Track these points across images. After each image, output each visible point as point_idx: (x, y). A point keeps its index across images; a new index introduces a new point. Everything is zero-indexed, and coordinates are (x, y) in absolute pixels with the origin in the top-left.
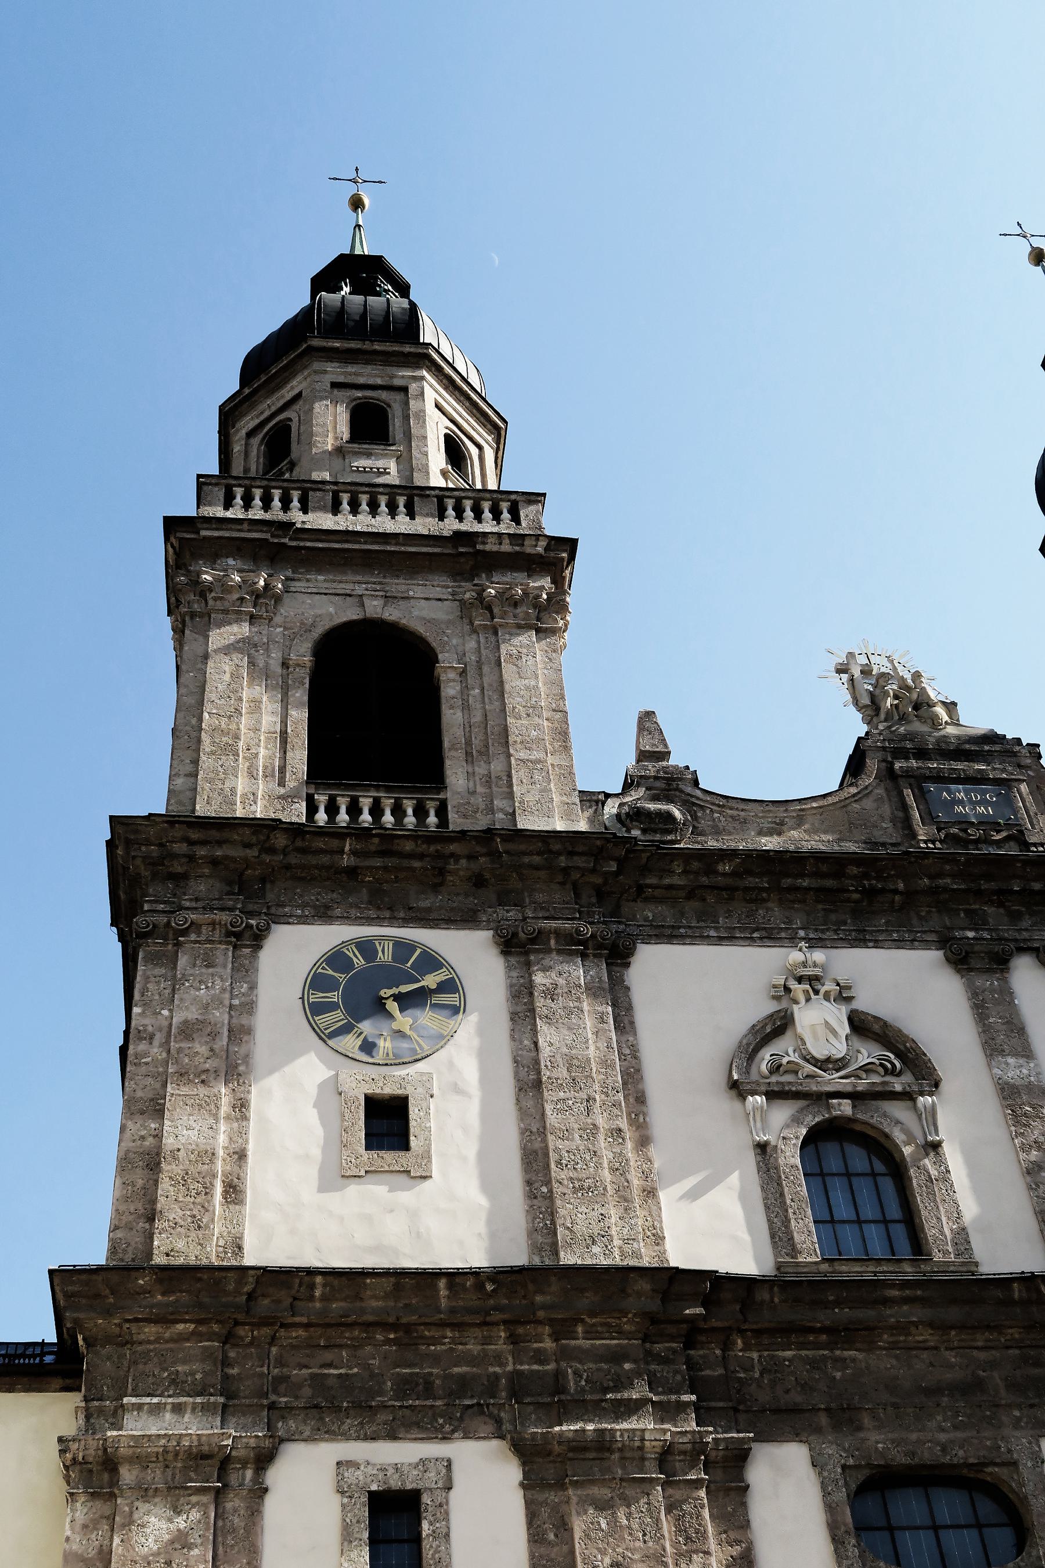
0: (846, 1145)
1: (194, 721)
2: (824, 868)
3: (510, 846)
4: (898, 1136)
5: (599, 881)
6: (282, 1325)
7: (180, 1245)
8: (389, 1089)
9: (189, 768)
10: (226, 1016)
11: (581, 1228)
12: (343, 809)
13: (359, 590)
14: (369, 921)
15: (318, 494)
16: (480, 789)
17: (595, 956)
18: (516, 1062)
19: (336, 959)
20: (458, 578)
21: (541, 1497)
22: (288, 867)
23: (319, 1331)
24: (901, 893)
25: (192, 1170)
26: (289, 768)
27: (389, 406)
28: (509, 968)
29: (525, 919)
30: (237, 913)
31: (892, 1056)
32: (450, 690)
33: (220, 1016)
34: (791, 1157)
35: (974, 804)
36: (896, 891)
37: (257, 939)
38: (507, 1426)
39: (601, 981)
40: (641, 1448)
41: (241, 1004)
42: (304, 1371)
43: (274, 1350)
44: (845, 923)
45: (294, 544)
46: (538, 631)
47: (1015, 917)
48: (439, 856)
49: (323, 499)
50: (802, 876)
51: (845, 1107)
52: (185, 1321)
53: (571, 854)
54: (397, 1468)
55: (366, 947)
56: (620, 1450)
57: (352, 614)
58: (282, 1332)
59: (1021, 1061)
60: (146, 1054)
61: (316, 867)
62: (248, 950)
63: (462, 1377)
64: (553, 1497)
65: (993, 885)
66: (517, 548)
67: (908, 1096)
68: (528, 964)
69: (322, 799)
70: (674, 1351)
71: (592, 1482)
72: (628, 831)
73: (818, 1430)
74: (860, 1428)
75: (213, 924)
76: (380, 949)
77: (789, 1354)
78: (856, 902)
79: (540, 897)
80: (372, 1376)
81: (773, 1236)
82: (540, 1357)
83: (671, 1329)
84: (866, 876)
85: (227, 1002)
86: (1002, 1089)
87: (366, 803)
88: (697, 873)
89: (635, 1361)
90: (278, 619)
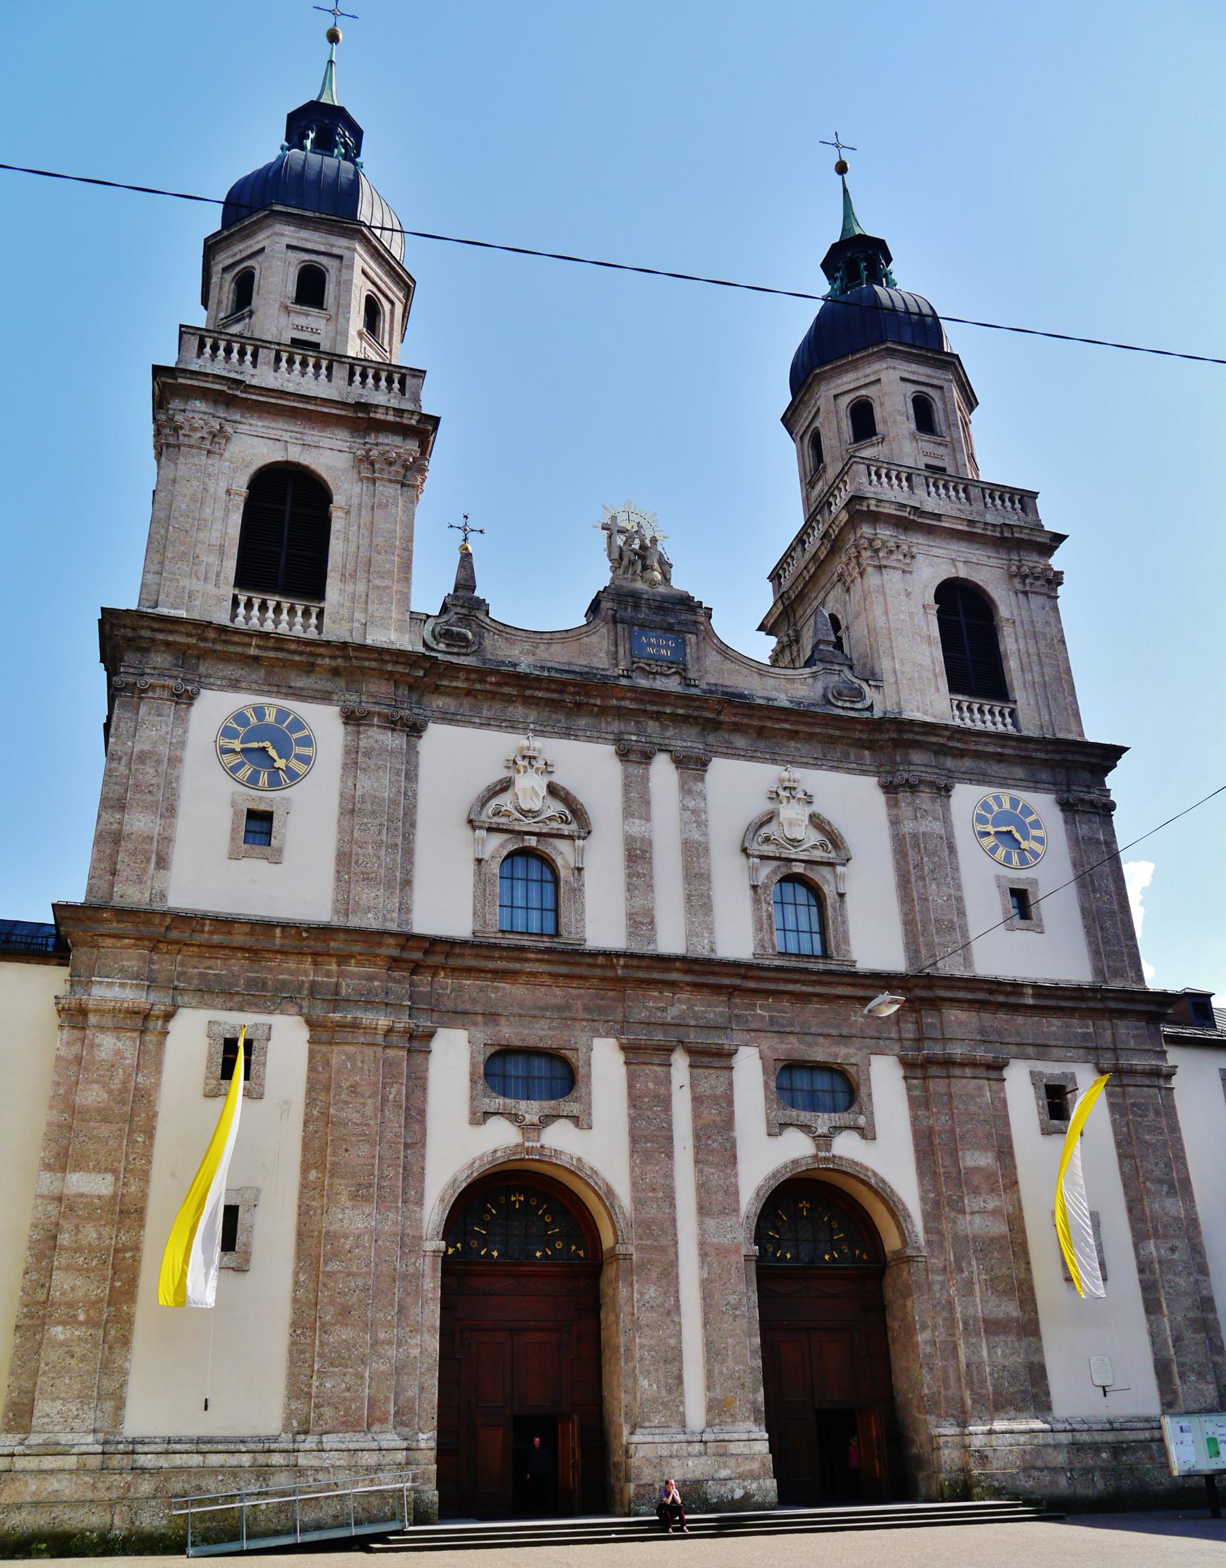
0: (530, 860)
1: (162, 531)
2: (553, 686)
3: (357, 654)
4: (559, 862)
5: (412, 681)
6: (185, 944)
7: (130, 891)
8: (262, 807)
9: (157, 568)
10: (167, 750)
11: (364, 903)
12: (256, 607)
13: (286, 436)
14: (262, 693)
15: (265, 351)
16: (347, 604)
17: (401, 731)
18: (341, 796)
19: (240, 718)
20: (355, 434)
21: (317, 1047)
22: (215, 651)
23: (206, 949)
24: (598, 706)
25: (139, 847)
26: (222, 575)
27: (328, 271)
28: (347, 734)
29: (361, 702)
30: (180, 681)
32: (337, 524)
33: (164, 750)
34: (495, 868)
36: (595, 705)
37: (191, 698)
38: (305, 1010)
39: (401, 749)
40: (376, 1029)
41: (178, 742)
42: (196, 970)
43: (179, 957)
44: (560, 721)
45: (244, 395)
46: (403, 485)
47: (664, 728)
48: (312, 654)
49: (268, 355)
50: (539, 689)
51: (532, 842)
52: (130, 938)
53: (396, 663)
55: (259, 711)
56: (364, 1028)
57: (278, 456)
58: (185, 948)
59: (643, 822)
60: (116, 770)
61: (233, 653)
62: (184, 706)
63: (284, 980)
64: (324, 1048)
65: (655, 708)
66: (398, 419)
67: (570, 837)
68: (359, 732)
69: (243, 599)
70: (404, 977)
71: (347, 1043)
72: (437, 644)
73: (476, 1024)
74: (498, 1025)
75: (164, 686)
76: (267, 713)
77: (468, 982)
78: (570, 708)
79: (373, 688)
80: (233, 976)
81: (474, 914)
82: (328, 974)
83: (404, 965)
84: (578, 693)
85: (168, 741)
86: (627, 839)
87: (271, 604)
88: (474, 681)
89: (381, 981)
90: (227, 455)
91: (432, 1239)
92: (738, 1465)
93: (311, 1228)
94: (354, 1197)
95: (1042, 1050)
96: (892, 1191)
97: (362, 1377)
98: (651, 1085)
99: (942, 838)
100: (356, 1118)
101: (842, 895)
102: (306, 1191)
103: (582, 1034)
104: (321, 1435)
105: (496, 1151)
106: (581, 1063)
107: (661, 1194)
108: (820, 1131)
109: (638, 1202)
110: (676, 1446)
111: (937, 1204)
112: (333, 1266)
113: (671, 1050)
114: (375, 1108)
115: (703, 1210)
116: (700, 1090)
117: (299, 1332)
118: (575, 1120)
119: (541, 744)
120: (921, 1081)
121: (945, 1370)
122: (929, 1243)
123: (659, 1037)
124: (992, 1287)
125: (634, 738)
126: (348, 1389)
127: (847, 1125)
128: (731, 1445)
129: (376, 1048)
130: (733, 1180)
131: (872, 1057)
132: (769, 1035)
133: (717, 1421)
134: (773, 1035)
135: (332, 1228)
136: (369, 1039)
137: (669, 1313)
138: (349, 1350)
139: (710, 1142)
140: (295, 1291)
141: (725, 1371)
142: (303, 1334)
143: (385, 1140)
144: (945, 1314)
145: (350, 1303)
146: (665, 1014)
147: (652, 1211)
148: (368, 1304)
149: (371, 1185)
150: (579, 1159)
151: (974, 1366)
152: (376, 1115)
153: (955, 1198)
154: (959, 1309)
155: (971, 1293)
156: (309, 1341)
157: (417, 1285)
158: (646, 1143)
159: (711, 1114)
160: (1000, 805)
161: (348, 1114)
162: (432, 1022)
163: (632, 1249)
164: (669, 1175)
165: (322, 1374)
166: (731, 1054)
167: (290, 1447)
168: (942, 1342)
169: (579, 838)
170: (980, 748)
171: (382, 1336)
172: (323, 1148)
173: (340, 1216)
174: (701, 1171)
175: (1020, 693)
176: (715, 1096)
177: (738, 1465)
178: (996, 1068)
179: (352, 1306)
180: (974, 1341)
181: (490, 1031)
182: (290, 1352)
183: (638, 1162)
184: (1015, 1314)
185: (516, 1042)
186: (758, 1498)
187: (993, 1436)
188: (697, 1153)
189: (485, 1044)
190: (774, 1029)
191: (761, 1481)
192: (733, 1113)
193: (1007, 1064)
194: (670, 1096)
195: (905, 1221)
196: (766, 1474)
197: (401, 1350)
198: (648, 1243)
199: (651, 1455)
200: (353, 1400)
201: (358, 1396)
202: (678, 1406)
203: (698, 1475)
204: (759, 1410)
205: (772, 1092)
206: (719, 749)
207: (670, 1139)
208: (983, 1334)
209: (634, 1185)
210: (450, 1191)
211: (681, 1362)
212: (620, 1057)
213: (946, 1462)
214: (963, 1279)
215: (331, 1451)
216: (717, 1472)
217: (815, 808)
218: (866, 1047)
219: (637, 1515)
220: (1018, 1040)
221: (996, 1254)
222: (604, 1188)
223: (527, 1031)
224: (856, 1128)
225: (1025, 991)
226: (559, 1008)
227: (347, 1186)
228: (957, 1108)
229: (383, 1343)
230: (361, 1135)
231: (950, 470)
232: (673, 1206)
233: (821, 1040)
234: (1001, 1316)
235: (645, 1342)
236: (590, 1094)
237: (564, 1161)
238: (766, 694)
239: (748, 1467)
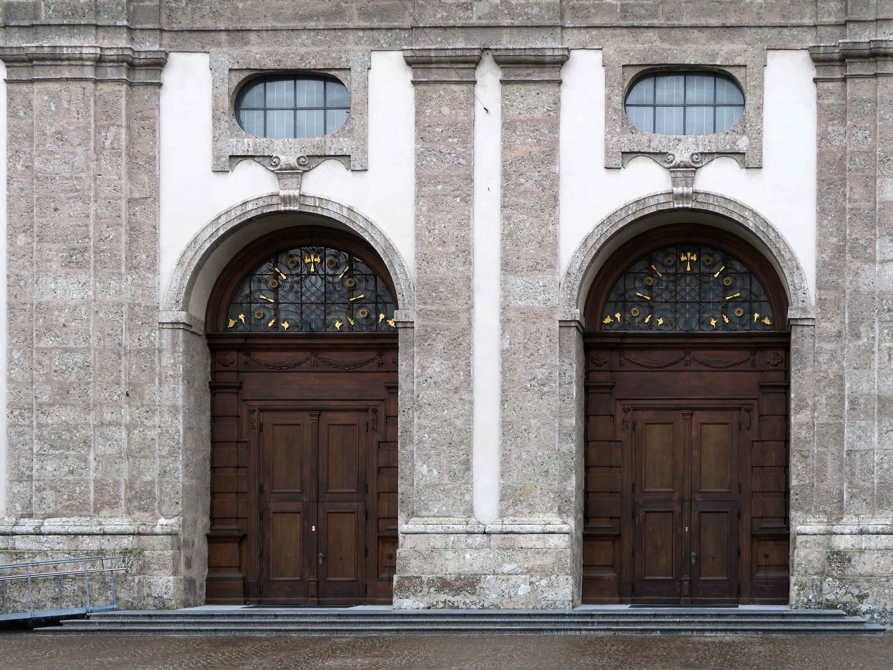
21: (16, 88)
74: (246, 44)
91: (170, 309)
92: (527, 559)
93: (22, 301)
94: (68, 263)
96: (778, 235)
97: (86, 460)
98: (446, 110)
100: (65, 170)
102: (13, 258)
103: (356, 48)
104: (44, 519)
105: (245, 203)
106: (354, 85)
107: (453, 249)
108: (678, 160)
109: (423, 259)
110: (452, 537)
111: (840, 251)
112: (47, 342)
113: (476, 63)
114: (88, 158)
115: (507, 267)
116: (513, 113)
117: (16, 413)
118: (344, 158)
120: (840, 84)
121: (822, 460)
122: (821, 302)
123: (459, 43)
126: (72, 472)
127: (721, 150)
129: (84, 84)
130: (551, 228)
131: (770, 53)
132: (618, 31)
134: (625, 31)
135: (45, 299)
136: (76, 73)
137: (457, 390)
138: (70, 432)
139: (522, 181)
140: (9, 370)
141: (524, 456)
142: (21, 415)
143: (103, 196)
144: (832, 391)
145: (68, 381)
146: (469, 13)
147: (441, 270)
148: (89, 383)
149: (86, 249)
150: (350, 209)
151: (858, 455)
152: (88, 167)
153: (862, 242)
154: (847, 385)
155: (868, 365)
156: (27, 422)
157: (153, 362)
158: (436, 185)
159: (527, 144)
161: (56, 167)
162: (161, 45)
163: (413, 317)
164: (465, 223)
165: (42, 456)
166: (560, 62)
167: (9, 529)
168: (821, 425)
171: (108, 417)
172: (30, 210)
173: (53, 286)
174: (507, 218)
176: (533, 119)
177: (527, 559)
179: (71, 384)
180: (863, 423)
181: (236, 52)
182: (8, 434)
183: (424, 209)
185: (270, 64)
187: (864, 537)
188: (504, 196)
189: (230, 70)
191: (553, 577)
192: (557, 141)
194: (472, 123)
195: (792, 274)
196: (562, 569)
197: (136, 432)
198: (435, 308)
200: (77, 483)
201: (83, 480)
202: (462, 494)
203: (476, 568)
204: (568, 501)
205: (615, 111)
207: (469, 179)
208: (876, 416)
209: (418, 237)
210: (190, 254)
211: (470, 446)
212: (407, 75)
213: (800, 564)
215: (50, 534)
216: (500, 566)
218: (761, 40)
222: (382, 244)
223: (283, 50)
227: (58, 251)
228: (882, 119)
229: (110, 424)
230: (72, 191)
232: (468, 262)
233: (695, 33)
235: (425, 422)
236: (365, 126)
237: (332, 212)
239: (539, 562)
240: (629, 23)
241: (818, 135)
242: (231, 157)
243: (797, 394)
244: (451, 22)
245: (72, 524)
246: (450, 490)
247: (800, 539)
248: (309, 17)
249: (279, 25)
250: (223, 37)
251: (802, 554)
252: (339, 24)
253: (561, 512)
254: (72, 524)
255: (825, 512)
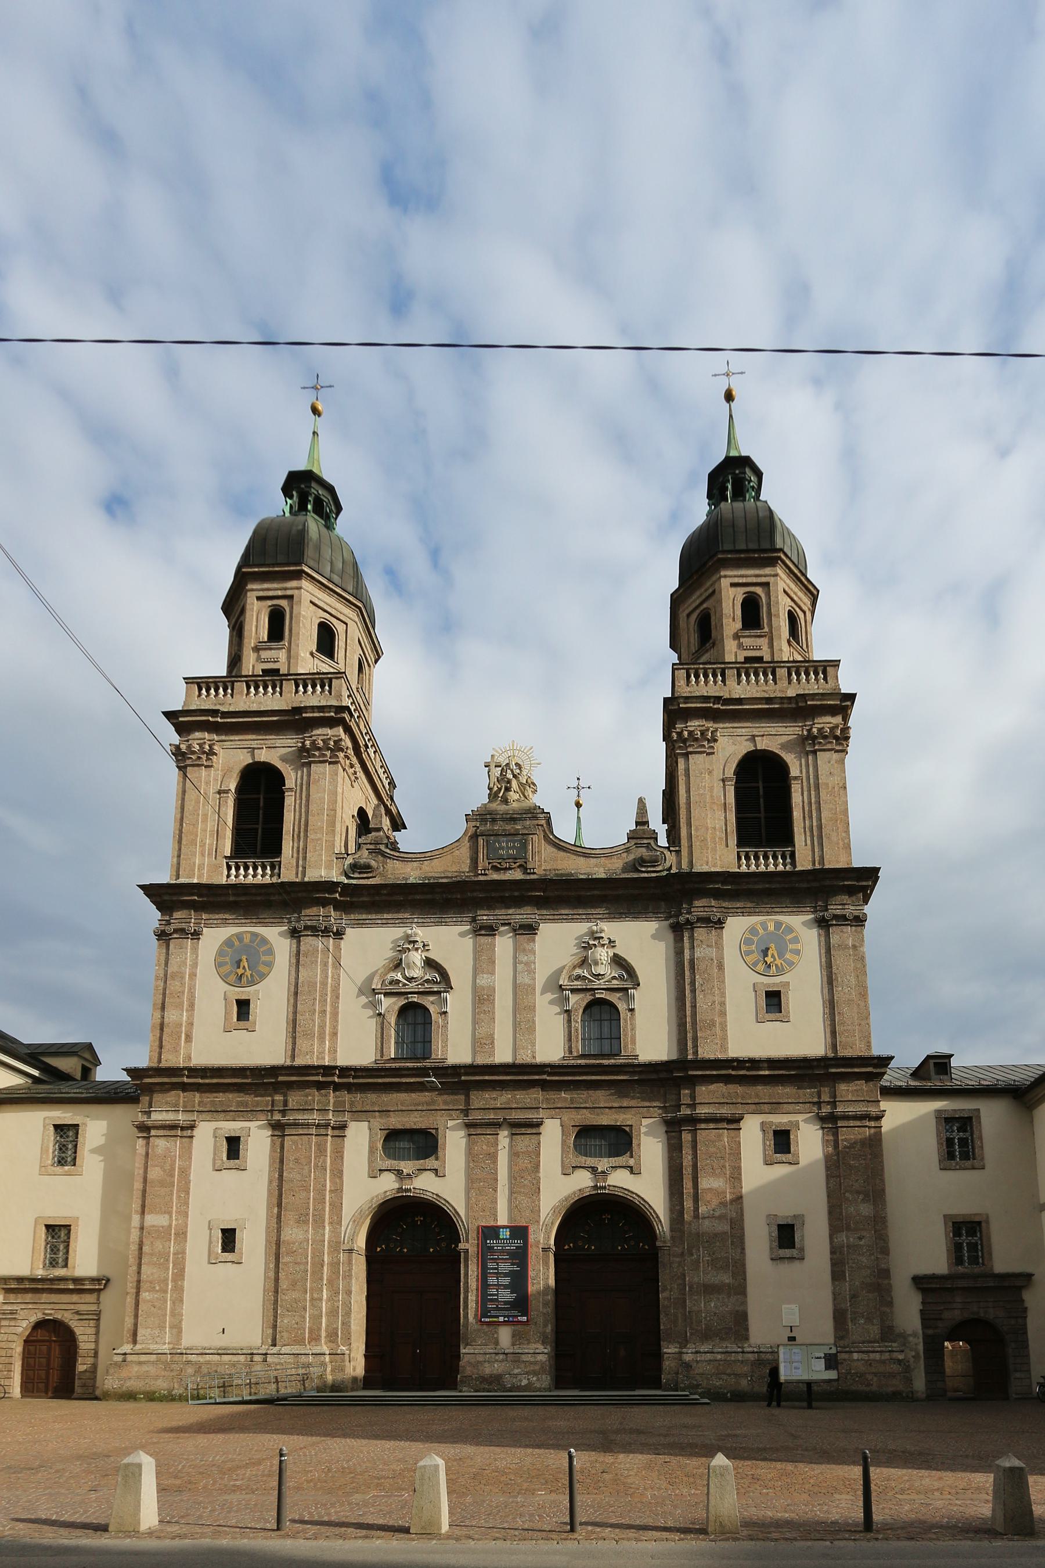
31: (437, 975)
35: (508, 848)
51: (415, 999)
54: (234, 1130)
59: (489, 976)
73: (375, 1117)
92: (526, 1367)
95: (775, 1107)
97: (304, 1317)
99: (712, 960)
101: (632, 1010)
105: (386, 1192)
119: (421, 933)
122: (672, 1237)
124: (712, 1265)
125: (485, 918)
127: (621, 1165)
128: (523, 1356)
133: (518, 1343)
144: (680, 1281)
150: (437, 1195)
154: (687, 1279)
160: (765, 929)
169: (444, 992)
170: (750, 886)
173: (290, 1232)
175: (799, 838)
177: (526, 1367)
178: (734, 1121)
180: (696, 1297)
181: (383, 1121)
184: (727, 1281)
186: (538, 1385)
189: (380, 1129)
190: (572, 1106)
193: (742, 1118)
199: (473, 1361)
200: (299, 1329)
202: (493, 1334)
204: (547, 1337)
206: (548, 917)
214: (692, 1260)
217: (617, 951)
219: (460, 1392)
220: (757, 1101)
221: (718, 1244)
224: (631, 1169)
225: (761, 1065)
226: (428, 1104)
228: (700, 1150)
229: (316, 1299)
231: (767, 658)
234: (717, 1282)
237: (428, 1196)
238: (588, 870)
239: (532, 1368)
240: (575, 1106)
241: (669, 1157)
242: (380, 1170)
243: (662, 1283)
244: (488, 1106)
245: (296, 1349)
246: (487, 1332)
247: (666, 1356)
248: (418, 1105)
249: (404, 1108)
250: (377, 1113)
251: (667, 1363)
252: (433, 1107)
253: (543, 1343)
254: (296, 1349)
255: (678, 1342)
